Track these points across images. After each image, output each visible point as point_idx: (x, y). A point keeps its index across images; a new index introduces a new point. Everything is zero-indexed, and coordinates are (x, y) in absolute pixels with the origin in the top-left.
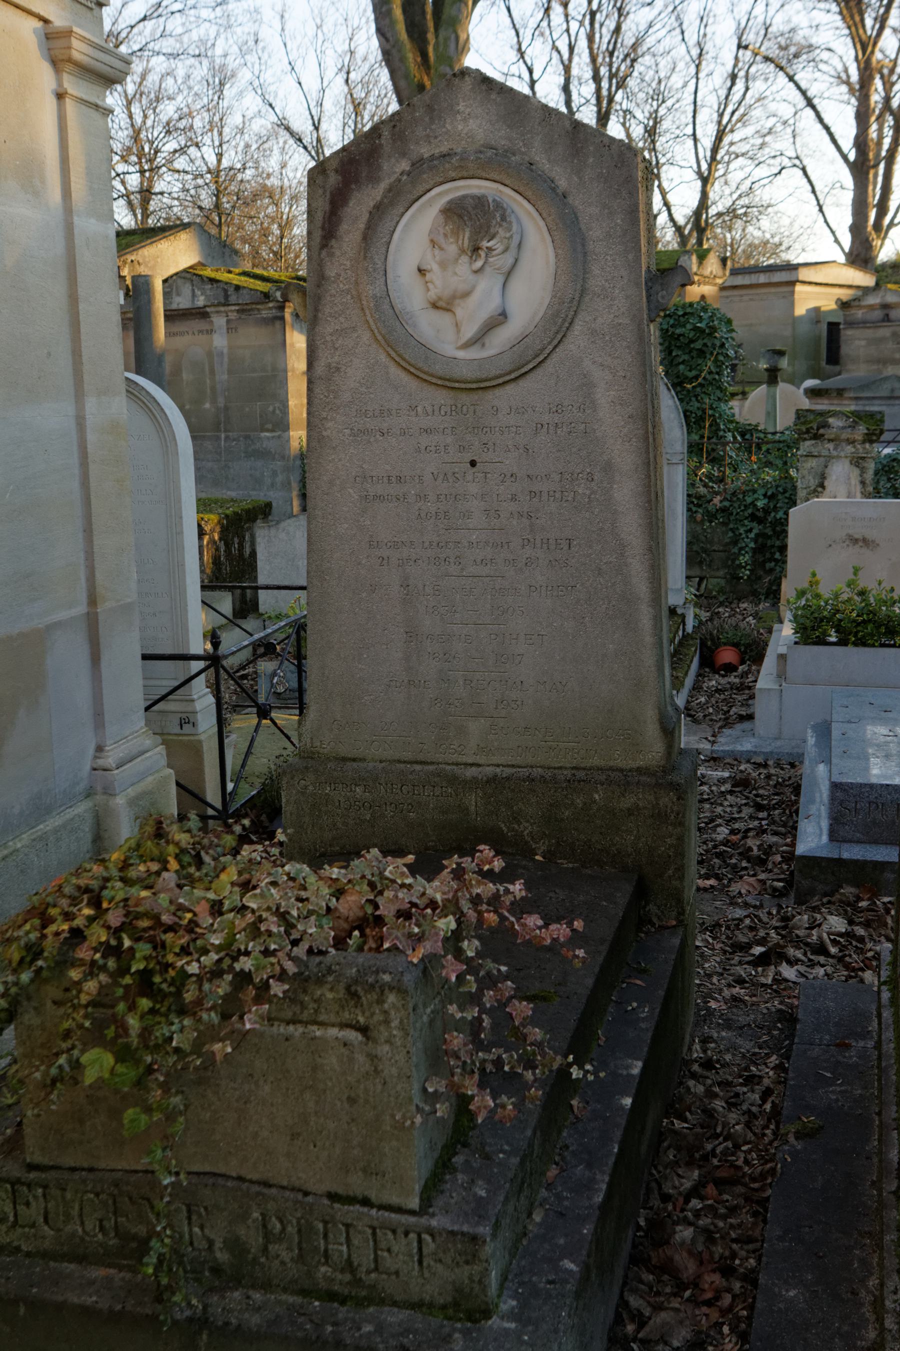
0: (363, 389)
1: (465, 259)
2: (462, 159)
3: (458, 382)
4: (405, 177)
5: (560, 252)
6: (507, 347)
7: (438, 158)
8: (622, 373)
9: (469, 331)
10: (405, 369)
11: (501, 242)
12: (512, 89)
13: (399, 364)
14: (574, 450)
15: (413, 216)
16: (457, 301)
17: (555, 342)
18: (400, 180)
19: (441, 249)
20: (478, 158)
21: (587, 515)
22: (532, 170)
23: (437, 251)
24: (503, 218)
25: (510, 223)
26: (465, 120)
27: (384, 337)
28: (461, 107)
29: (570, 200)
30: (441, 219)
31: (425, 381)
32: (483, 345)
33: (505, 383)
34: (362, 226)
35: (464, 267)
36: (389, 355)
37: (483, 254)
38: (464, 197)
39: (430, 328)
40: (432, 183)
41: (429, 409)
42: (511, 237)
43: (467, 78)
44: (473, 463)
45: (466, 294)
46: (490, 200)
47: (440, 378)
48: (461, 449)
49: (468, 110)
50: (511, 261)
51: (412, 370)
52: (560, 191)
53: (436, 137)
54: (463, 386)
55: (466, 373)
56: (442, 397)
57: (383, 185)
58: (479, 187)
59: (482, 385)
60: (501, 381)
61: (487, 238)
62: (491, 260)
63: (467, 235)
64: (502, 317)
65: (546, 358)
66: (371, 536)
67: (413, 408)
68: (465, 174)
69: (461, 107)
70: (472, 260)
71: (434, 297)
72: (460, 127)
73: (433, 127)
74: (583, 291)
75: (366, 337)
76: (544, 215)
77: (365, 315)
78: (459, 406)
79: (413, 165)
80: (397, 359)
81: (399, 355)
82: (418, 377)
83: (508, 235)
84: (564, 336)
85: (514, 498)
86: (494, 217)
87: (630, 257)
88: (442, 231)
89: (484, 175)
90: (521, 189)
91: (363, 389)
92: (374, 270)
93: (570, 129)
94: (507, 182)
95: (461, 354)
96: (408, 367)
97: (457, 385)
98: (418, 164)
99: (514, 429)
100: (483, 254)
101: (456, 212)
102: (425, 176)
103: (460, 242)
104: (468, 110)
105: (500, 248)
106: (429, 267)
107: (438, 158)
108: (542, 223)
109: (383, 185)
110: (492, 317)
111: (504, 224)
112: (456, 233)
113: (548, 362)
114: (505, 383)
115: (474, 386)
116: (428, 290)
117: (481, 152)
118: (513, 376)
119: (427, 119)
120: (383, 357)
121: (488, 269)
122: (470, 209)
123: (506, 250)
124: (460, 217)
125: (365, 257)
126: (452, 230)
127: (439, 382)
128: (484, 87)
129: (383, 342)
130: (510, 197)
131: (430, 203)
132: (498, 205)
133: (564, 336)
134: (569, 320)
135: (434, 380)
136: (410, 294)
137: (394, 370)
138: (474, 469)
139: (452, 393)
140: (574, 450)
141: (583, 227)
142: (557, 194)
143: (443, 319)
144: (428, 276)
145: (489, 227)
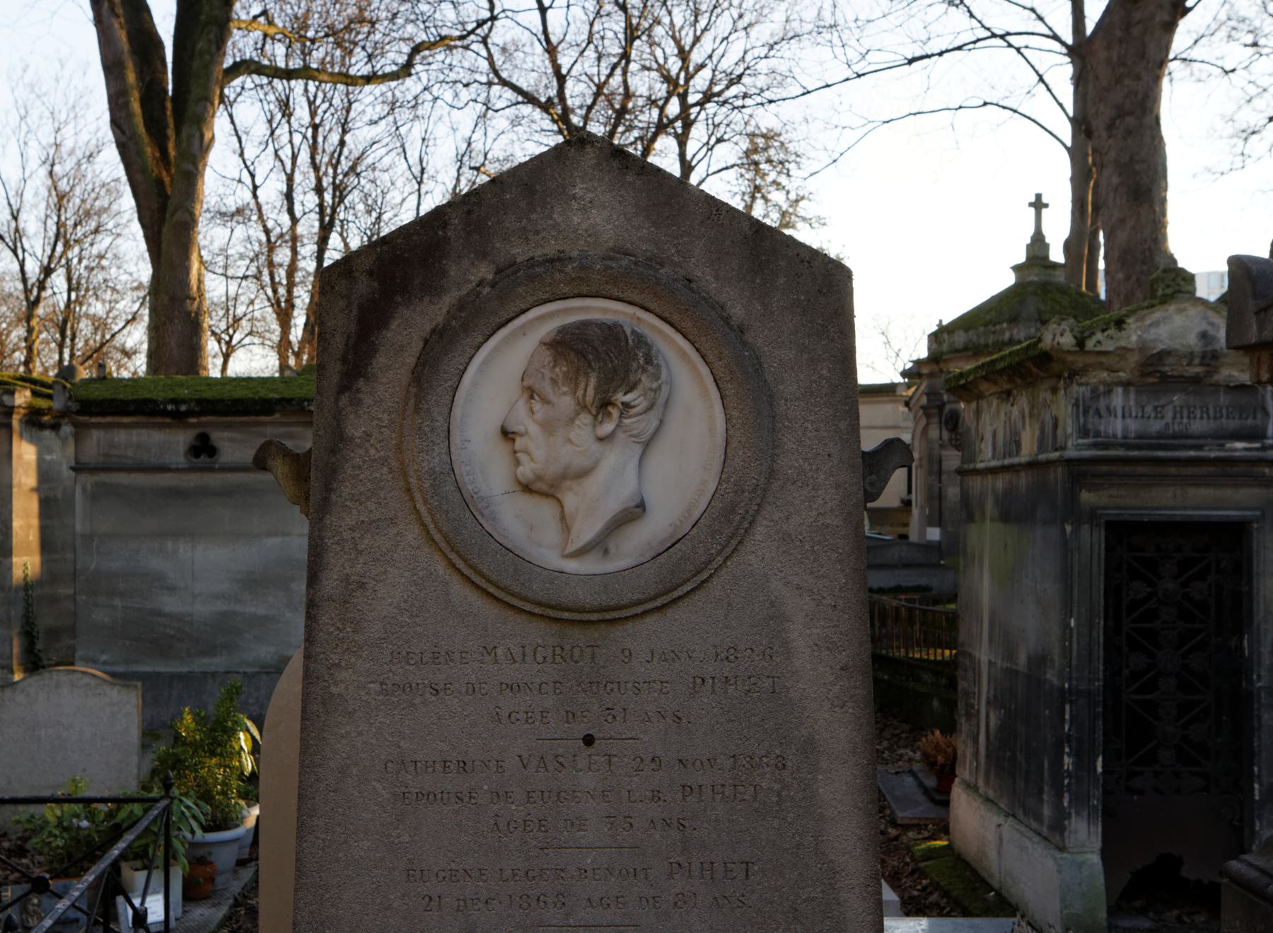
0: (405, 618)
1: (585, 418)
2: (582, 268)
3: (569, 610)
4: (487, 290)
5: (735, 413)
6: (648, 557)
7: (540, 264)
8: (829, 601)
9: (586, 531)
10: (478, 587)
11: (645, 395)
12: (659, 170)
13: (468, 579)
14: (754, 719)
15: (497, 349)
16: (568, 483)
17: (728, 551)
18: (478, 294)
19: (545, 401)
20: (607, 268)
21: (776, 823)
22: (692, 290)
23: (537, 406)
24: (649, 360)
25: (658, 366)
26: (584, 209)
27: (445, 537)
28: (577, 191)
29: (749, 337)
30: (547, 356)
31: (513, 607)
32: (606, 552)
33: (646, 613)
34: (411, 361)
35: (583, 431)
36: (454, 566)
37: (615, 413)
38: (586, 324)
39: (525, 527)
40: (531, 300)
41: (517, 651)
42: (659, 388)
43: (588, 149)
44: (589, 740)
45: (584, 473)
46: (628, 333)
47: (540, 604)
48: (571, 715)
49: (590, 195)
50: (655, 423)
51: (491, 590)
52: (735, 321)
53: (537, 233)
54: (577, 616)
55: (584, 596)
56: (537, 633)
57: (448, 300)
58: (604, 310)
59: (608, 616)
60: (639, 609)
61: (624, 388)
62: (626, 421)
63: (593, 382)
64: (636, 511)
65: (711, 576)
66: (411, 861)
67: (489, 650)
68: (585, 290)
69: (577, 191)
70: (596, 421)
71: (530, 475)
72: (576, 220)
73: (534, 216)
74: (772, 474)
75: (412, 534)
76: (711, 358)
77: (412, 499)
78: (567, 647)
79: (499, 271)
80: (467, 571)
81: (472, 567)
82: (489, 594)
83: (655, 385)
84: (741, 542)
85: (656, 796)
86: (635, 357)
87: (843, 425)
88: (548, 374)
89: (616, 293)
90: (676, 318)
91: (405, 618)
92: (432, 430)
93: (749, 233)
94: (651, 306)
95: (572, 566)
96: (485, 585)
97: (566, 615)
98: (506, 270)
99: (657, 686)
100: (615, 413)
101: (572, 347)
102: (520, 290)
103: (580, 393)
104: (590, 195)
105: (642, 403)
106: (522, 428)
107: (540, 264)
108: (704, 370)
109: (448, 300)
110: (625, 510)
111: (650, 368)
112: (573, 379)
113: (715, 580)
114: (646, 613)
115: (595, 617)
116: (518, 463)
117: (610, 258)
118: (659, 602)
119: (523, 204)
120: (441, 568)
121: (621, 436)
122: (597, 343)
123: (649, 408)
124: (581, 354)
125: (417, 410)
126: (566, 375)
127: (537, 610)
128: (615, 164)
129: (443, 545)
130: (653, 327)
131: (523, 330)
132: (640, 340)
133: (741, 542)
134: (749, 518)
135: (528, 607)
136: (484, 467)
137: (459, 590)
138: (591, 750)
139: (556, 627)
140: (754, 719)
141: (770, 378)
142: (731, 328)
143: (544, 511)
144: (520, 443)
145: (627, 372)
